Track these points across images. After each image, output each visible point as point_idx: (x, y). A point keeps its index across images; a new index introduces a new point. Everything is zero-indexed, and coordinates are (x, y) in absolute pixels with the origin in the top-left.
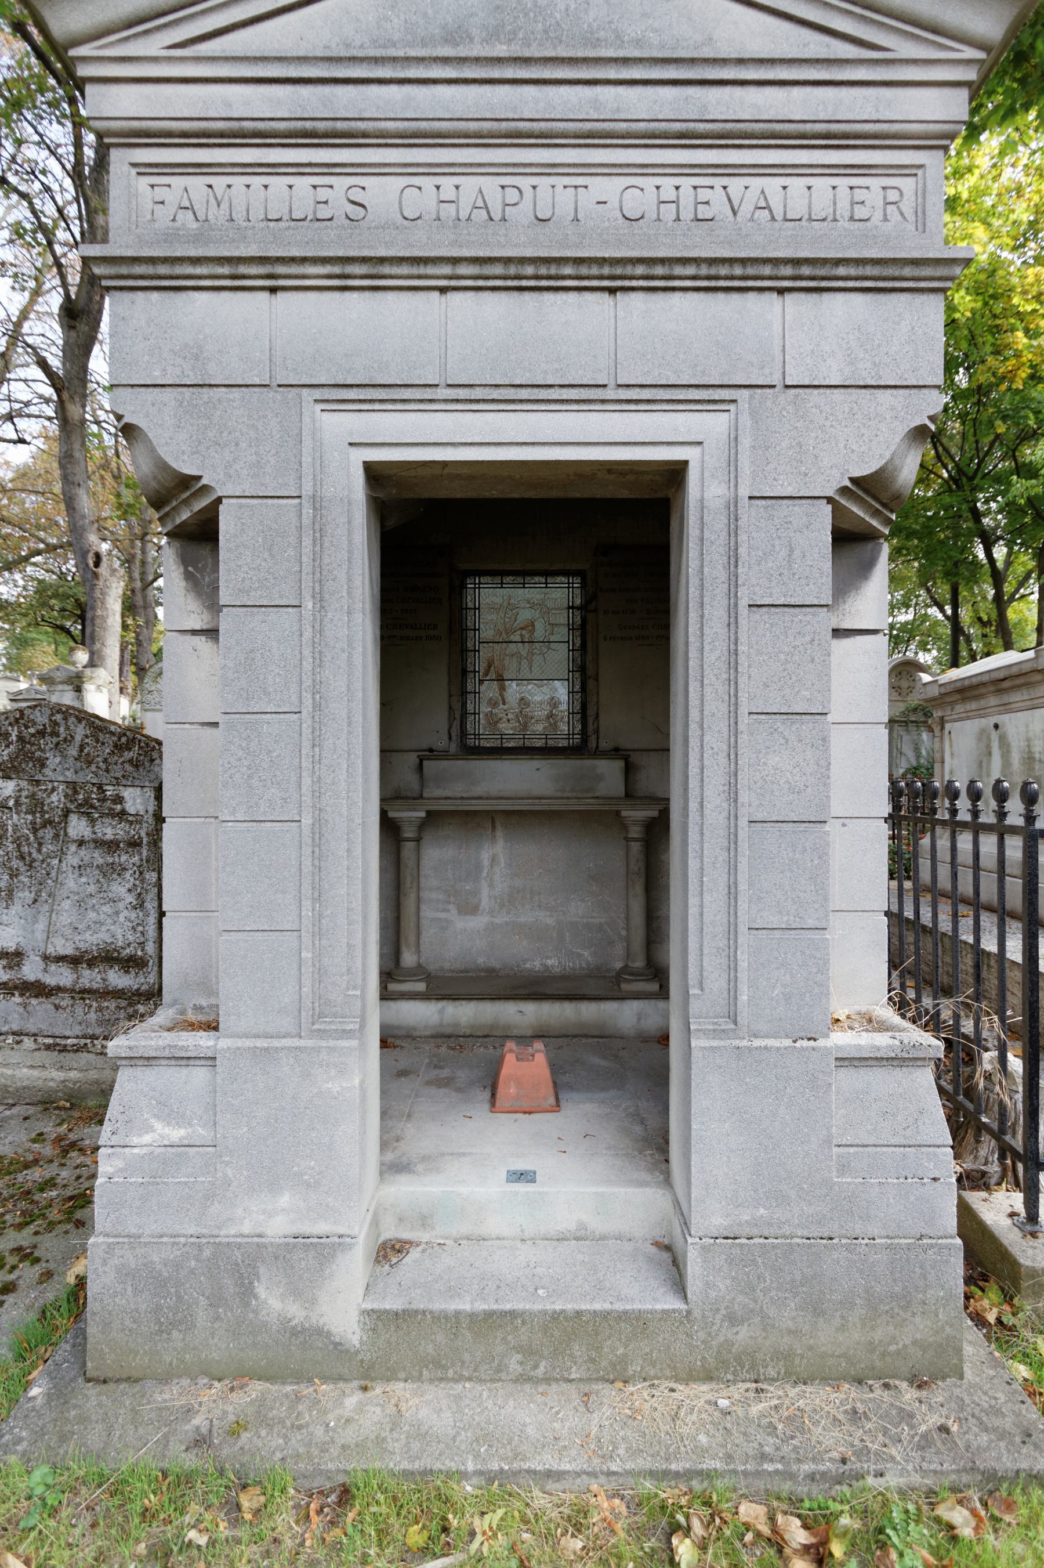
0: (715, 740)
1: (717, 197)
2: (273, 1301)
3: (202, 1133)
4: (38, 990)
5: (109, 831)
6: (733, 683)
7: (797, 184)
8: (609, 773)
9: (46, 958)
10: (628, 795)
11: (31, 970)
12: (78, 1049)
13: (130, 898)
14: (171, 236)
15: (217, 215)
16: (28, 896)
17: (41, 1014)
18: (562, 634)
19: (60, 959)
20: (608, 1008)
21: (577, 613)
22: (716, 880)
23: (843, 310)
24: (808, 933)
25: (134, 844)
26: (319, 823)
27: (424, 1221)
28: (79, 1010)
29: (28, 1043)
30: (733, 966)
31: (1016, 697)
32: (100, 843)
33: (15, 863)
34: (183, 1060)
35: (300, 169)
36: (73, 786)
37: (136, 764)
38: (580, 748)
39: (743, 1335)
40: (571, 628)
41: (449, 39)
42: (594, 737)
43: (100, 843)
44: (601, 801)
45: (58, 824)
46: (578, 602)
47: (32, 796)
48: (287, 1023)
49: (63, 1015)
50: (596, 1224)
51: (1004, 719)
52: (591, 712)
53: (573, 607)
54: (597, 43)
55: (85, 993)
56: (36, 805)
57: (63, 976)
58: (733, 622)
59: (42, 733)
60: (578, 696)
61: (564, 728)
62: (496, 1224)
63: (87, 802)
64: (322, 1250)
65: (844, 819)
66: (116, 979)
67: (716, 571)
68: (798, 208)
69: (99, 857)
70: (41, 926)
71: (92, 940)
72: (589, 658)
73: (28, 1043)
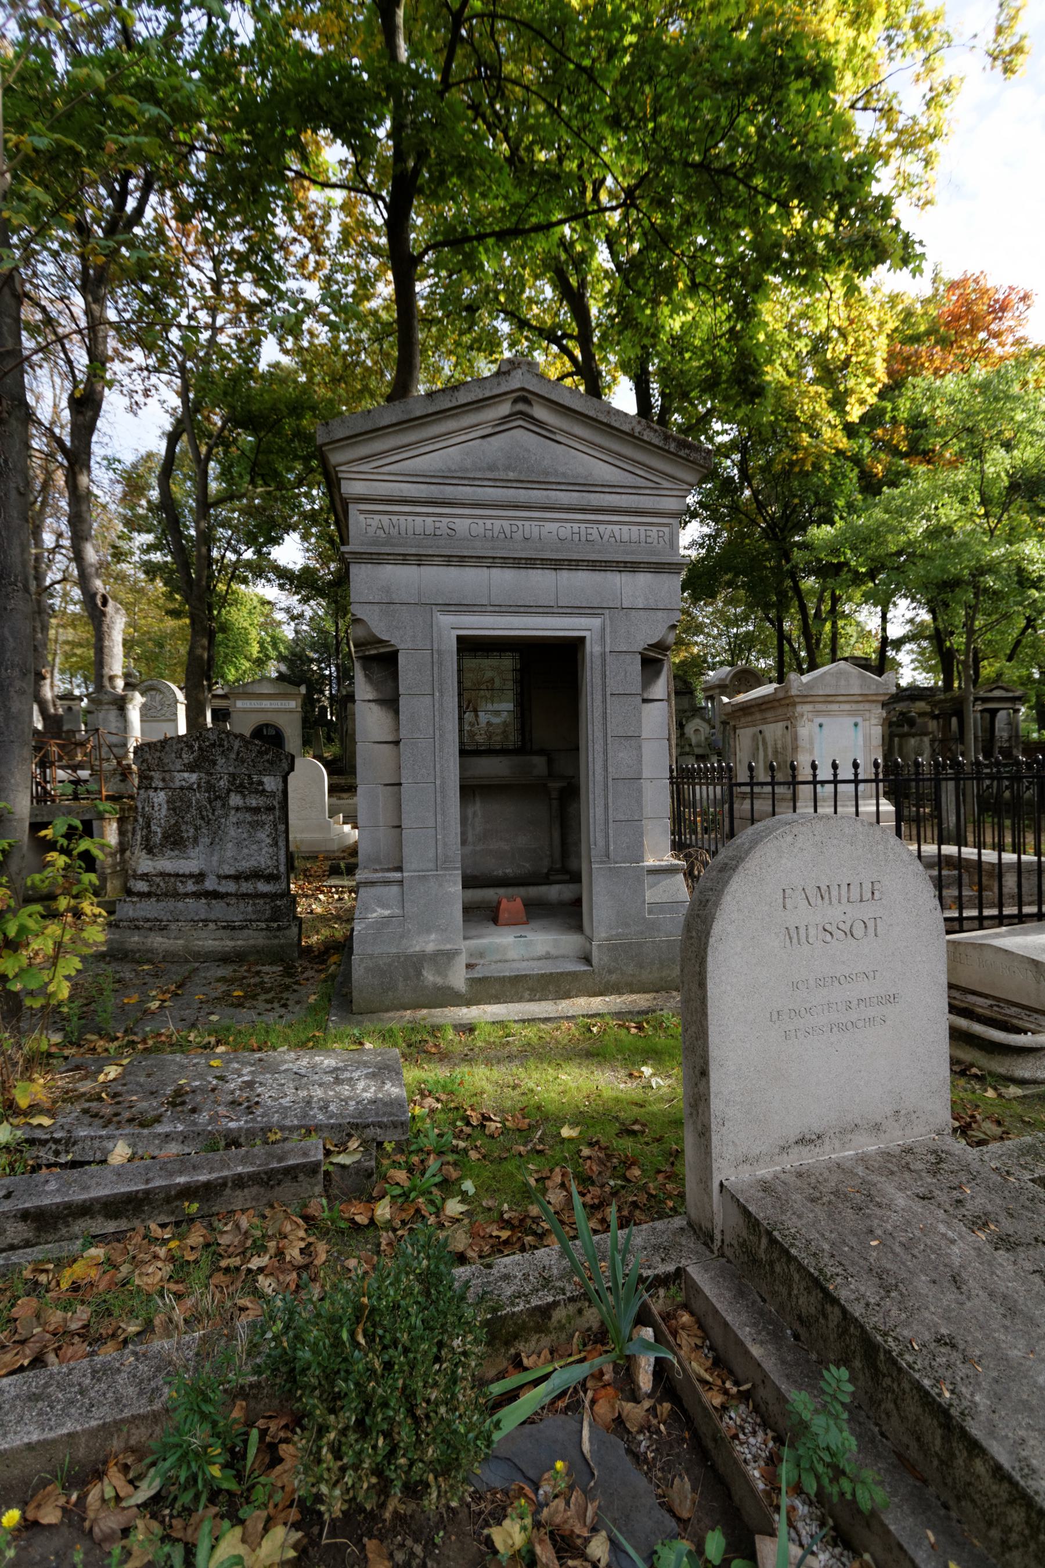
0: (599, 747)
1: (595, 532)
2: (430, 977)
3: (397, 912)
4: (215, 895)
5: (253, 802)
6: (605, 724)
7: (625, 528)
8: (539, 763)
9: (219, 877)
10: (550, 775)
11: (210, 884)
12: (242, 928)
13: (268, 841)
14: (375, 542)
15: (394, 532)
16: (207, 841)
17: (219, 909)
18: (510, 685)
19: (227, 877)
20: (543, 889)
22: (600, 802)
23: (643, 579)
24: (634, 824)
25: (270, 809)
26: (443, 783)
27: (481, 955)
28: (242, 905)
29: (212, 926)
30: (607, 836)
31: (769, 715)
32: (249, 809)
33: (199, 822)
34: (387, 883)
35: (428, 515)
36: (233, 776)
37: (271, 762)
38: (520, 751)
39: (614, 977)
40: (515, 682)
41: (492, 468)
43: (249, 809)
45: (224, 800)
48: (431, 865)
49: (232, 909)
50: (554, 952)
51: (764, 727)
54: (547, 474)
55: (244, 896)
56: (210, 787)
57: (230, 887)
58: (604, 701)
59: (213, 745)
62: (512, 954)
63: (242, 785)
64: (450, 956)
65: (652, 779)
66: (263, 887)
67: (597, 680)
68: (625, 538)
69: (248, 817)
70: (215, 858)
71: (245, 865)
73: (212, 926)
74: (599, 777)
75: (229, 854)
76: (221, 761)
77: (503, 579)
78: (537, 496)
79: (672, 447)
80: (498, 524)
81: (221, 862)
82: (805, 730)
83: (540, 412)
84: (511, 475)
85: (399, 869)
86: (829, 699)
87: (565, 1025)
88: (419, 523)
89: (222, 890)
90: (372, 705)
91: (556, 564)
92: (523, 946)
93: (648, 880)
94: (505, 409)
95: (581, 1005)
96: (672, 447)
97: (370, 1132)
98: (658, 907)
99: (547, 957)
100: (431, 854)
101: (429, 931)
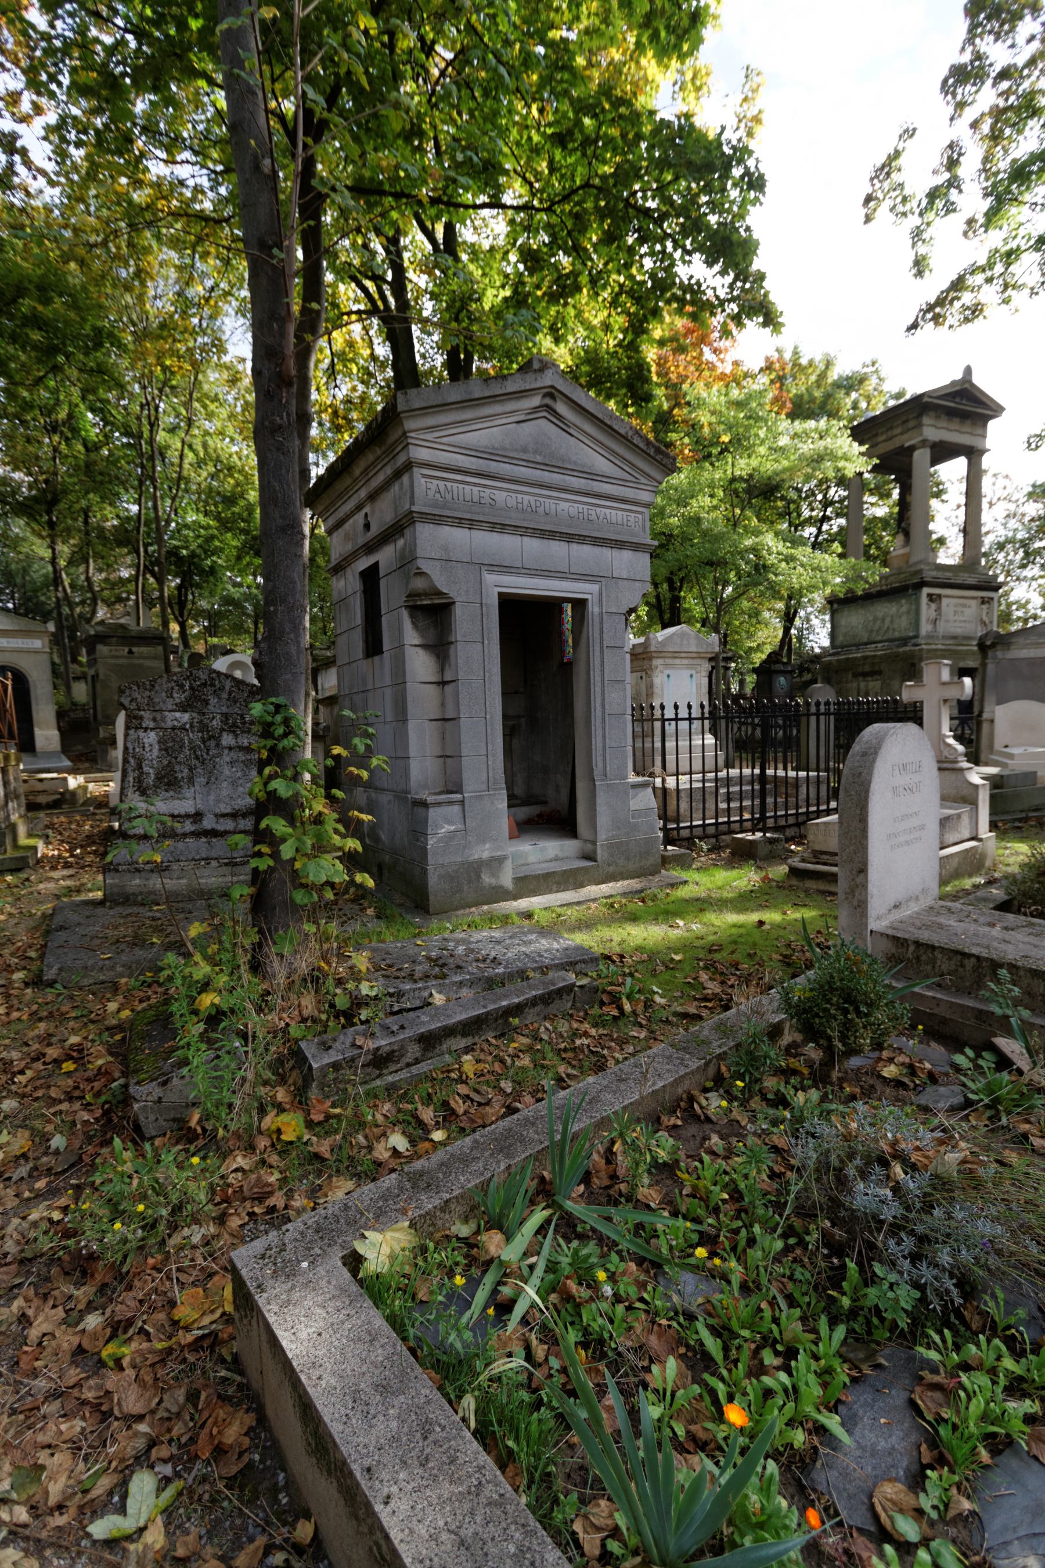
2: (487, 879)
4: (213, 833)
6: (602, 671)
11: (208, 823)
14: (435, 505)
16: (203, 780)
17: (219, 847)
19: (224, 815)
23: (627, 555)
29: (214, 863)
32: (241, 748)
33: (194, 762)
34: (450, 803)
35: (475, 485)
36: (226, 716)
41: (524, 450)
43: (241, 748)
45: (217, 739)
47: (201, 722)
48: (484, 787)
56: (203, 727)
57: (228, 825)
59: (204, 685)
62: (532, 859)
63: (234, 725)
64: (500, 860)
67: (597, 635)
69: (242, 756)
73: (214, 863)
74: (599, 713)
75: (225, 793)
76: (213, 701)
77: (532, 544)
78: (556, 478)
79: (652, 452)
80: (527, 498)
81: (218, 801)
82: (658, 680)
83: (561, 408)
84: (539, 459)
85: (459, 791)
86: (676, 655)
87: (593, 905)
88: (469, 490)
89: (220, 828)
90: (421, 651)
91: (569, 538)
92: (545, 852)
93: (631, 792)
94: (536, 401)
95: (593, 890)
96: (652, 452)
97: (578, 967)
98: (638, 813)
99: (556, 859)
100: (484, 778)
101: (484, 842)
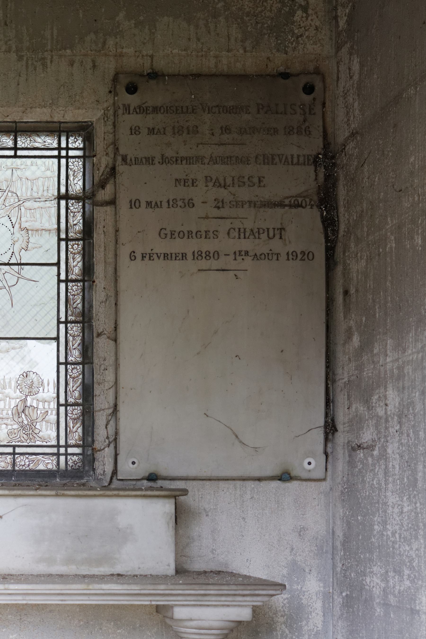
10: (180, 571)
18: (46, 247)
21: (76, 207)
38: (77, 475)
42: (108, 452)
44: (135, 588)
46: (77, 185)
52: (102, 401)
53: (67, 197)
60: (76, 371)
61: (48, 432)
72: (99, 295)
